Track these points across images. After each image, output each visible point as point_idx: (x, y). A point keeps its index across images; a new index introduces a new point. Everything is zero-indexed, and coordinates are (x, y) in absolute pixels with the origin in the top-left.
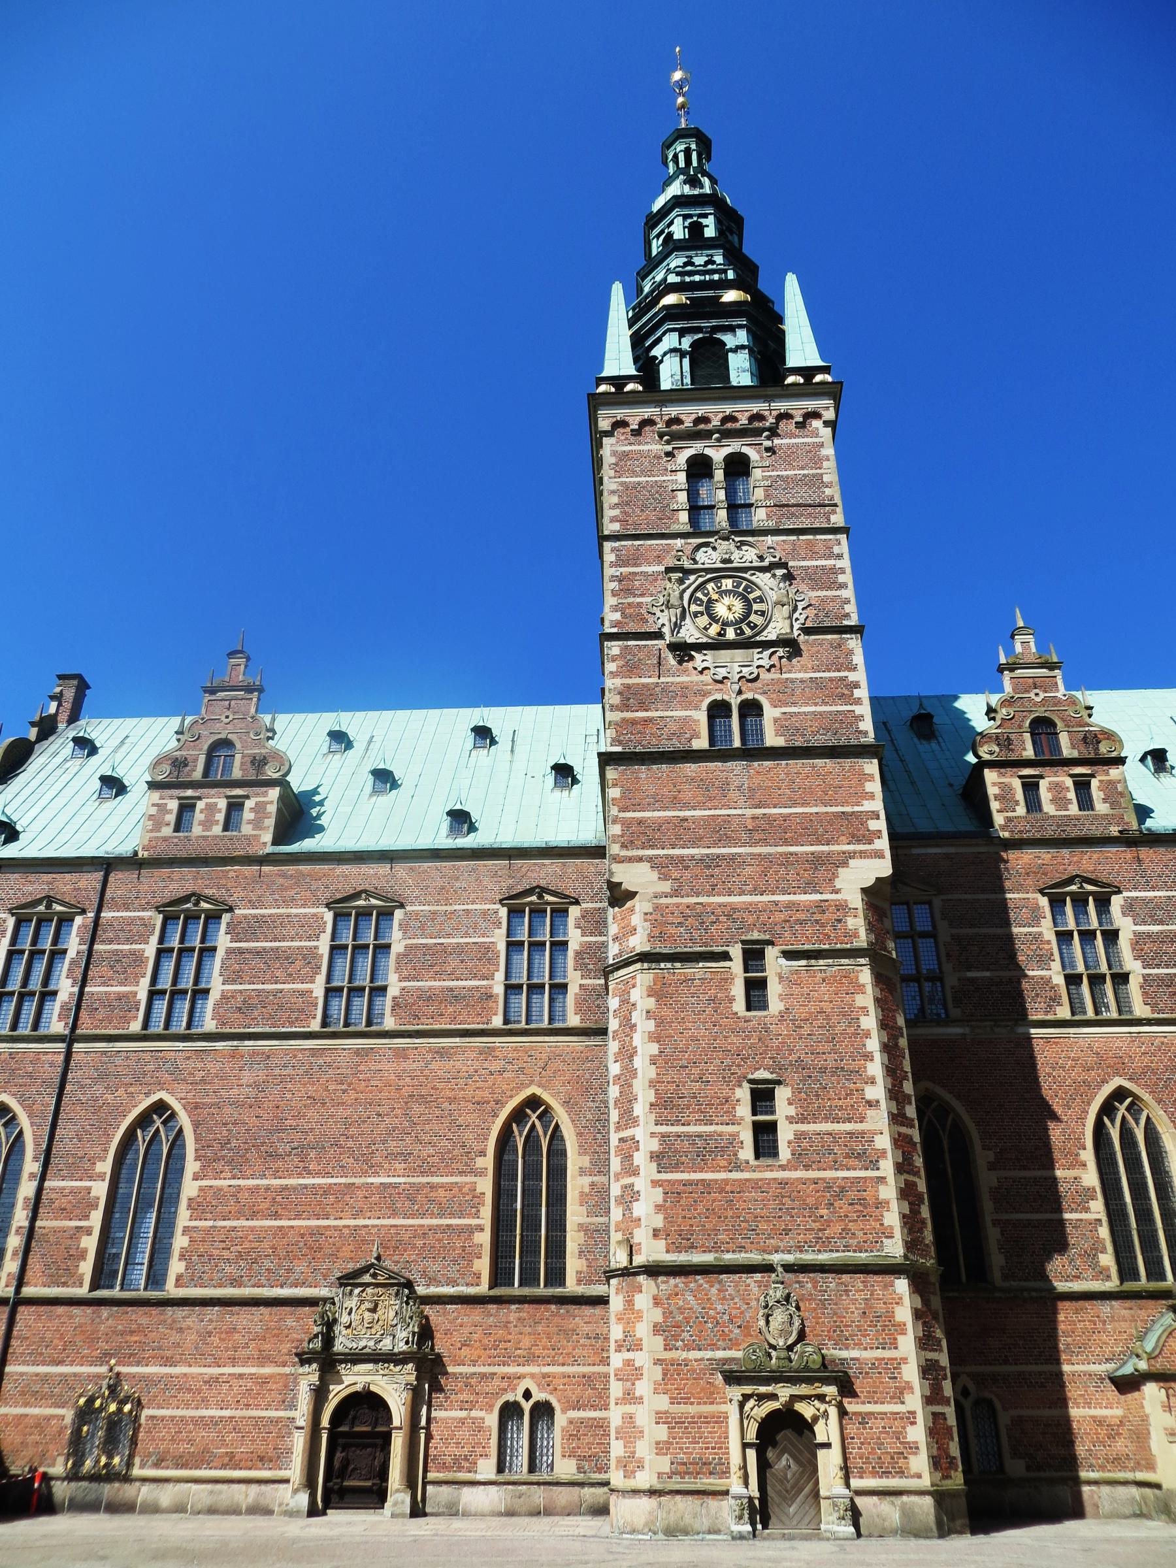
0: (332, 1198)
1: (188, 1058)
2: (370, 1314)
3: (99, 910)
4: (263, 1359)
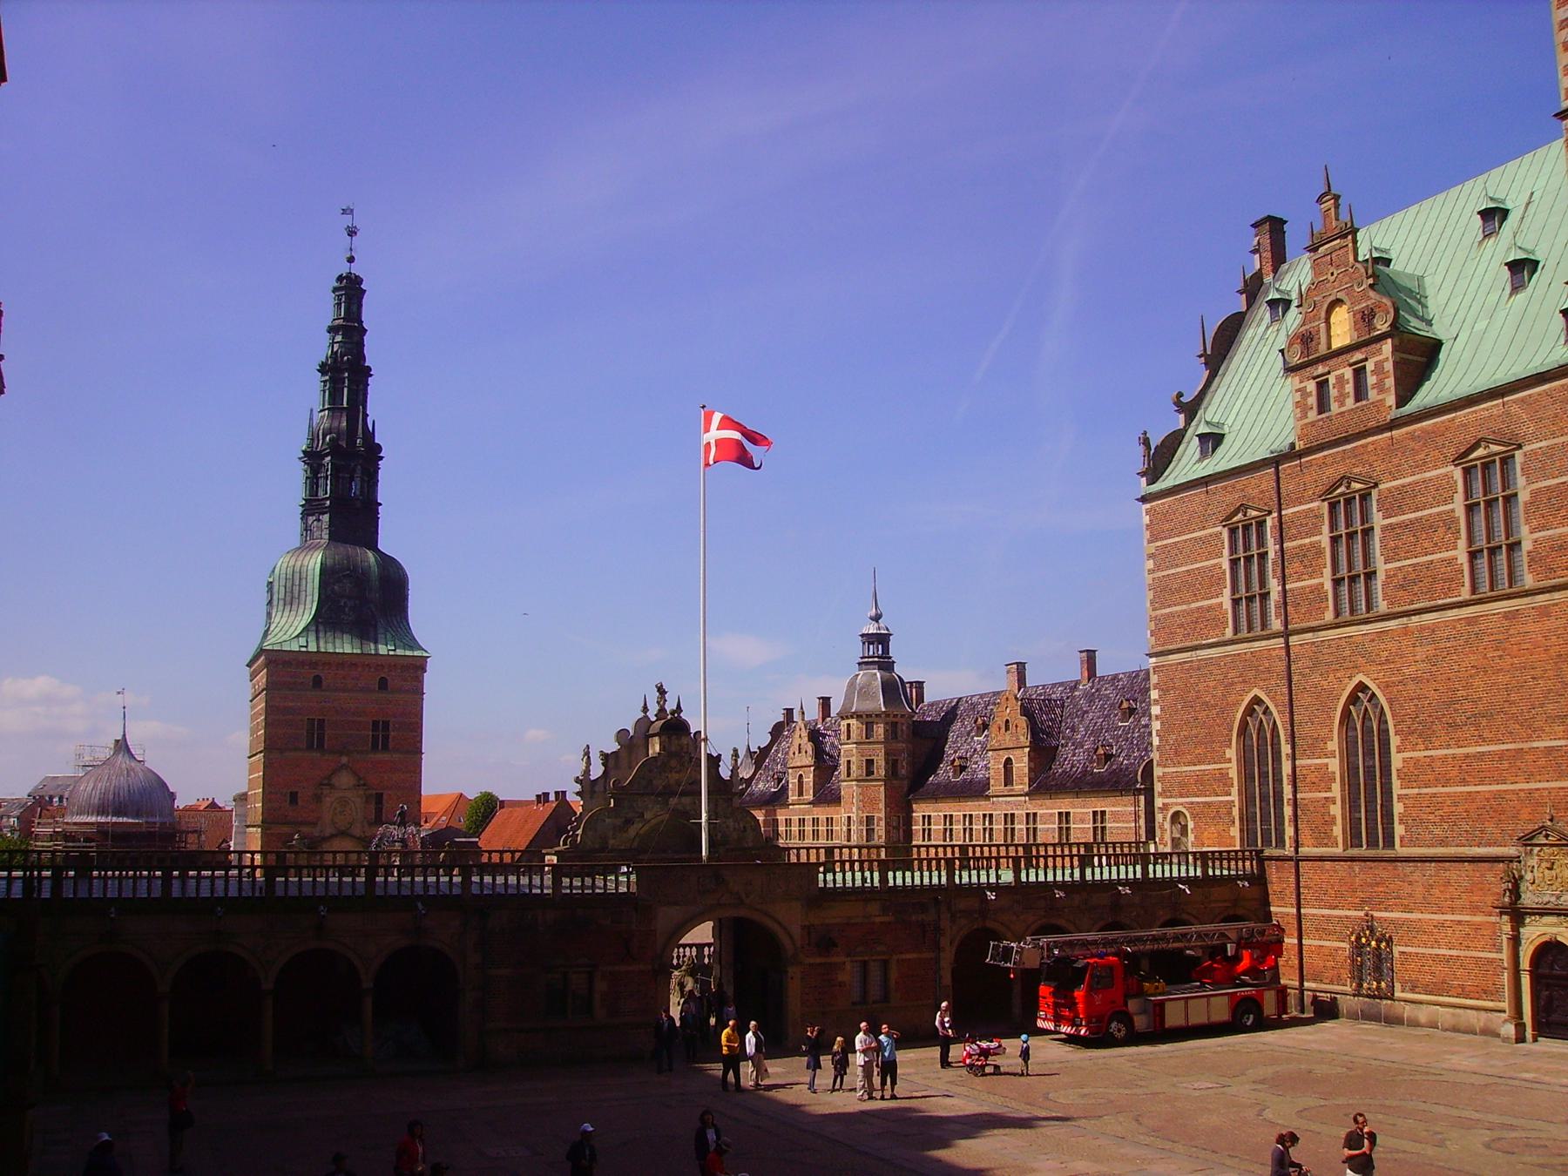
0: (1506, 765)
1: (1373, 640)
2: (1550, 872)
3: (1280, 510)
4: (1474, 909)
